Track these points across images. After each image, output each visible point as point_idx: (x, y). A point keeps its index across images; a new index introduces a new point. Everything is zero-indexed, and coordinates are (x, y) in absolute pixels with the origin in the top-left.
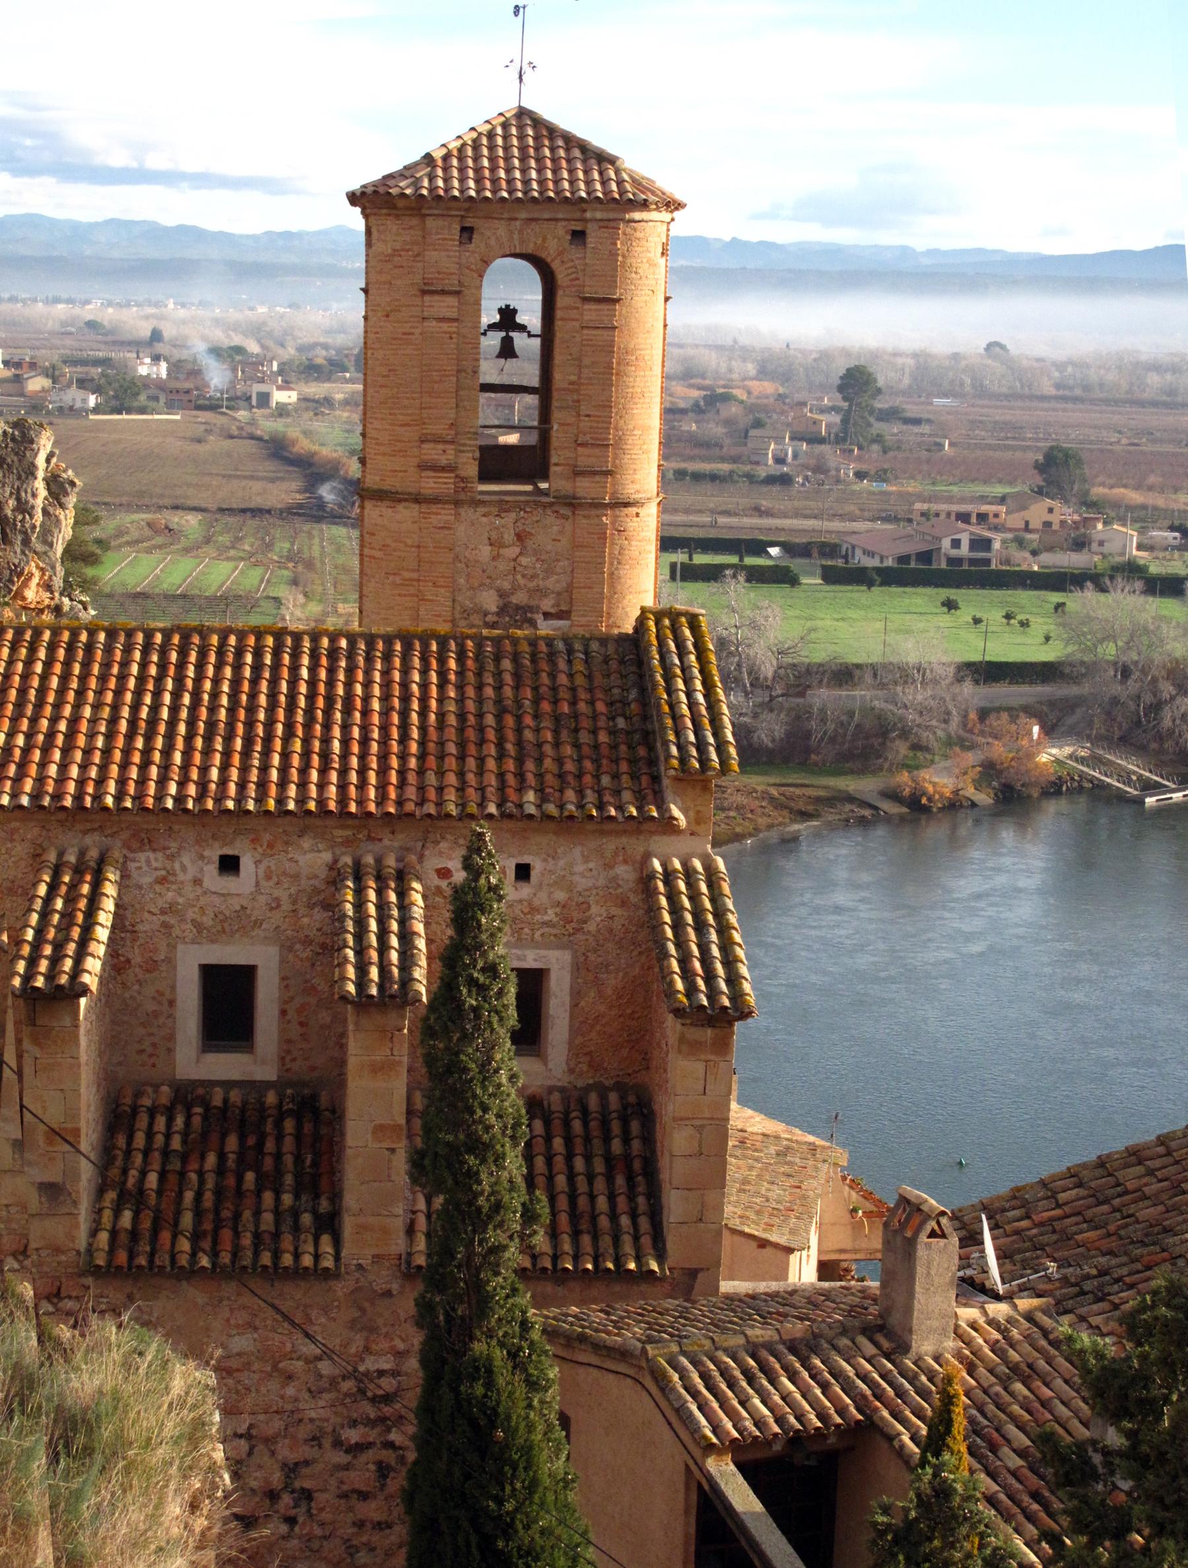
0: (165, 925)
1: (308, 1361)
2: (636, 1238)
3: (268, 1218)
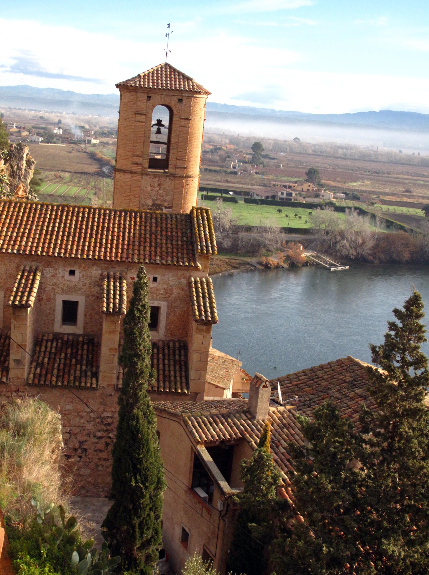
0: (53, 289)
1: (87, 413)
2: (181, 383)
3: (78, 373)
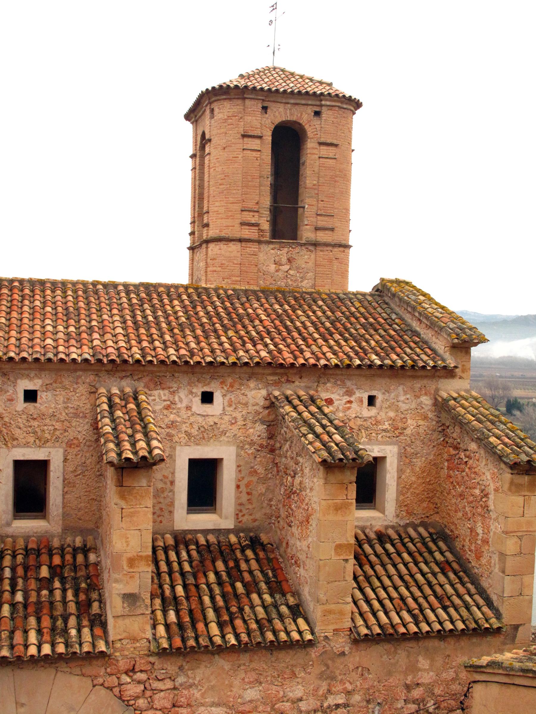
1: (293, 702)
3: (260, 610)
